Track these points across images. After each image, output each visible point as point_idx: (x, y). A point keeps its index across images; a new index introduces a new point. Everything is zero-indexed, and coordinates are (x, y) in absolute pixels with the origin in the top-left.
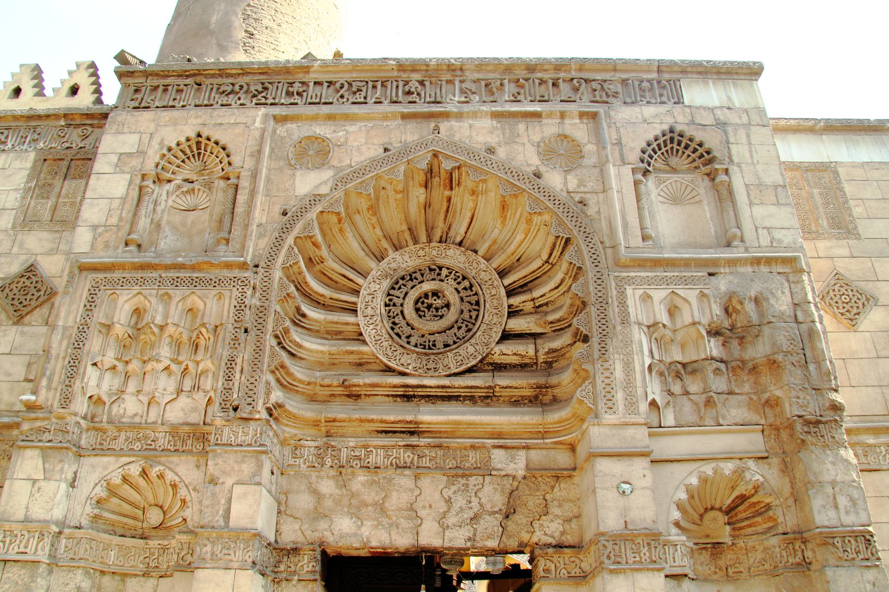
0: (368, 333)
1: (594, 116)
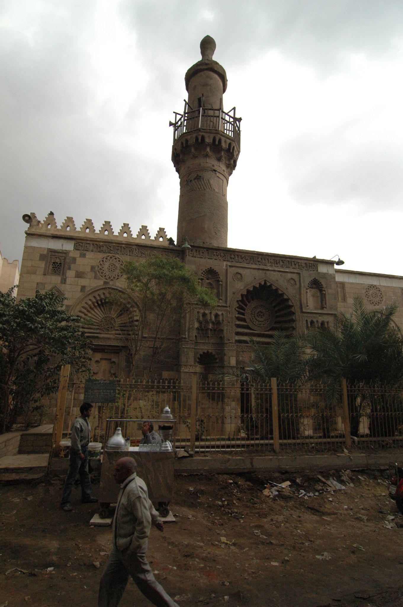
0: (248, 320)
1: (299, 274)
